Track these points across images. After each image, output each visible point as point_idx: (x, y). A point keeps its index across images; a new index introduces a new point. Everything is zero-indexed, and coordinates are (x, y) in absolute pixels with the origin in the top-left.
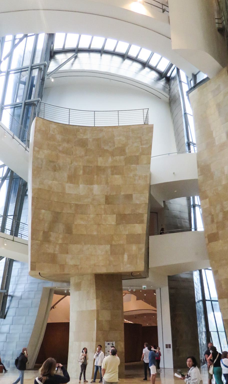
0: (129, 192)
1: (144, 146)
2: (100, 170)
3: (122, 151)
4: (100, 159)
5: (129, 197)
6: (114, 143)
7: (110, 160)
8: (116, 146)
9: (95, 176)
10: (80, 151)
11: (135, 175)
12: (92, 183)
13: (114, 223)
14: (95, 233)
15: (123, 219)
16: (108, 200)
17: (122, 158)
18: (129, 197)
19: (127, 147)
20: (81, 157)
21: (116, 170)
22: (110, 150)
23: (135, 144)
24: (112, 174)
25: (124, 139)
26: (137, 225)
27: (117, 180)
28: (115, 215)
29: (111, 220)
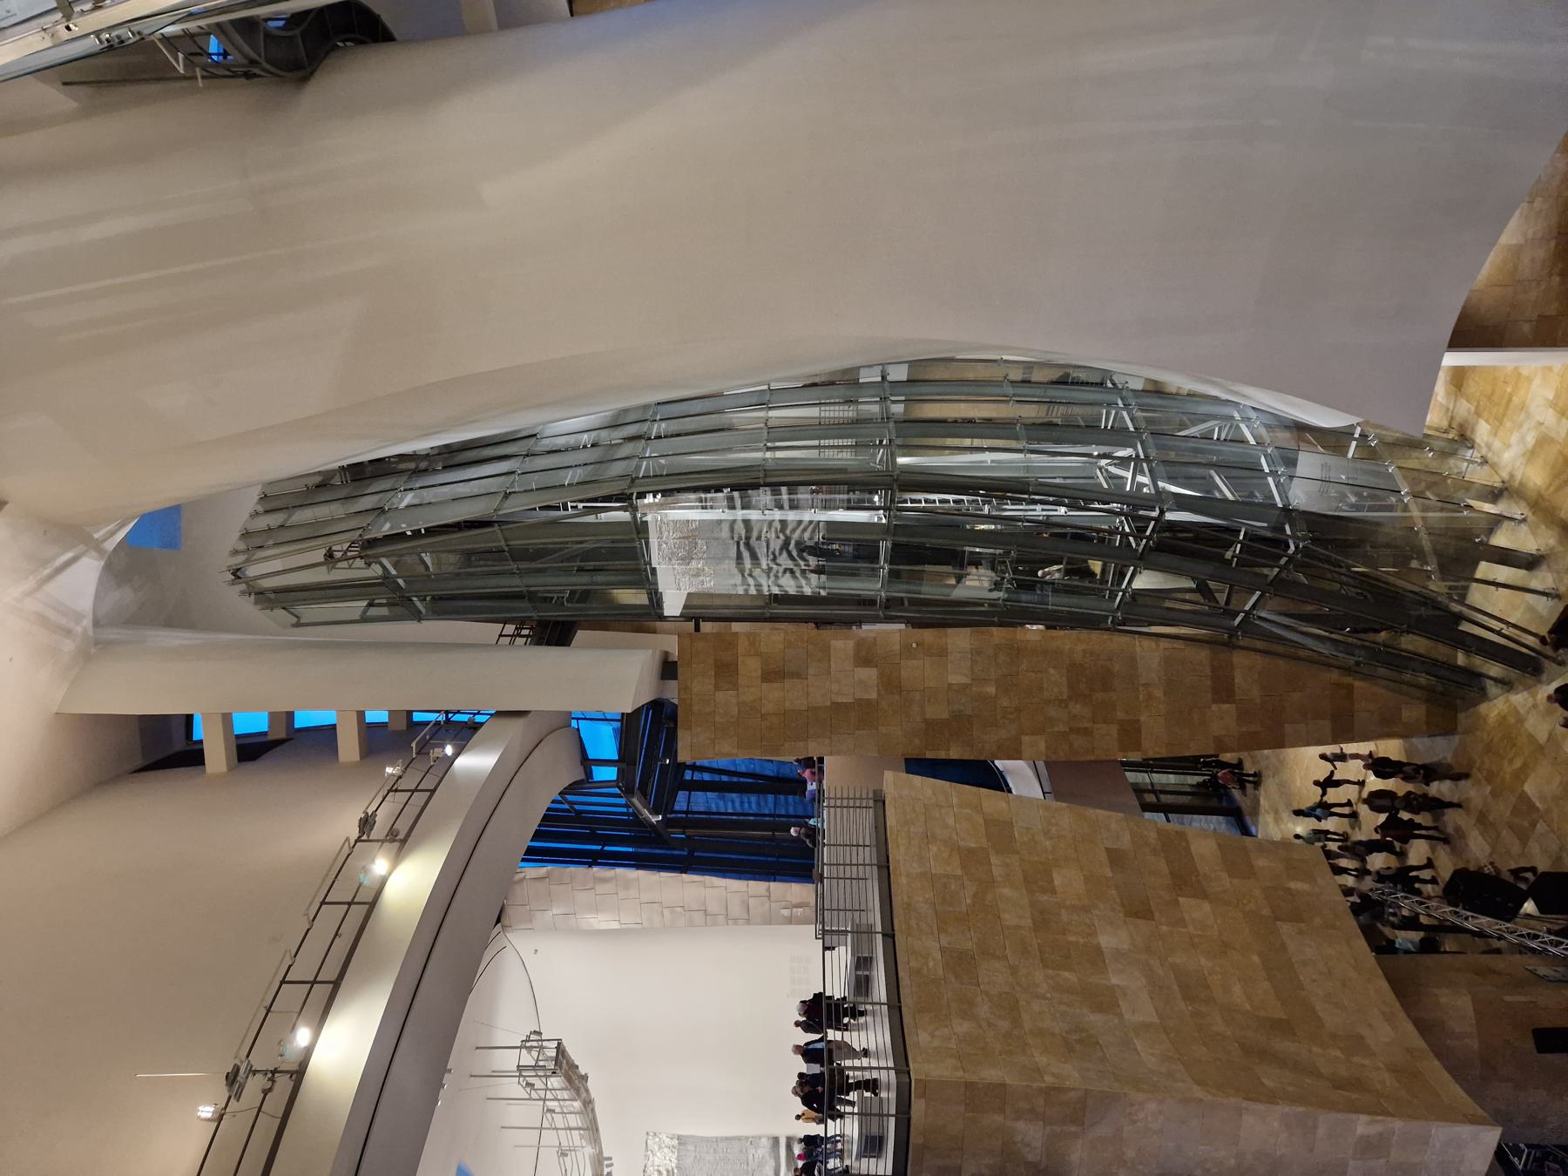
0: (1103, 856)
1: (955, 801)
2: (1043, 920)
3: (970, 858)
4: (1009, 918)
5: (1116, 858)
6: (947, 876)
7: (1006, 891)
8: (959, 872)
9: (1071, 938)
10: (994, 976)
11: (1046, 833)
12: (1098, 950)
13: (1207, 907)
14: (1255, 959)
15: (1186, 880)
16: (1138, 910)
17: (994, 860)
18: (1116, 858)
19: (962, 843)
20: (1014, 971)
21: (1037, 879)
22: (971, 888)
23: (951, 821)
24: (1054, 892)
25: (934, 849)
26: (1193, 848)
27: (1068, 880)
28: (1181, 899)
29: (1197, 911)
